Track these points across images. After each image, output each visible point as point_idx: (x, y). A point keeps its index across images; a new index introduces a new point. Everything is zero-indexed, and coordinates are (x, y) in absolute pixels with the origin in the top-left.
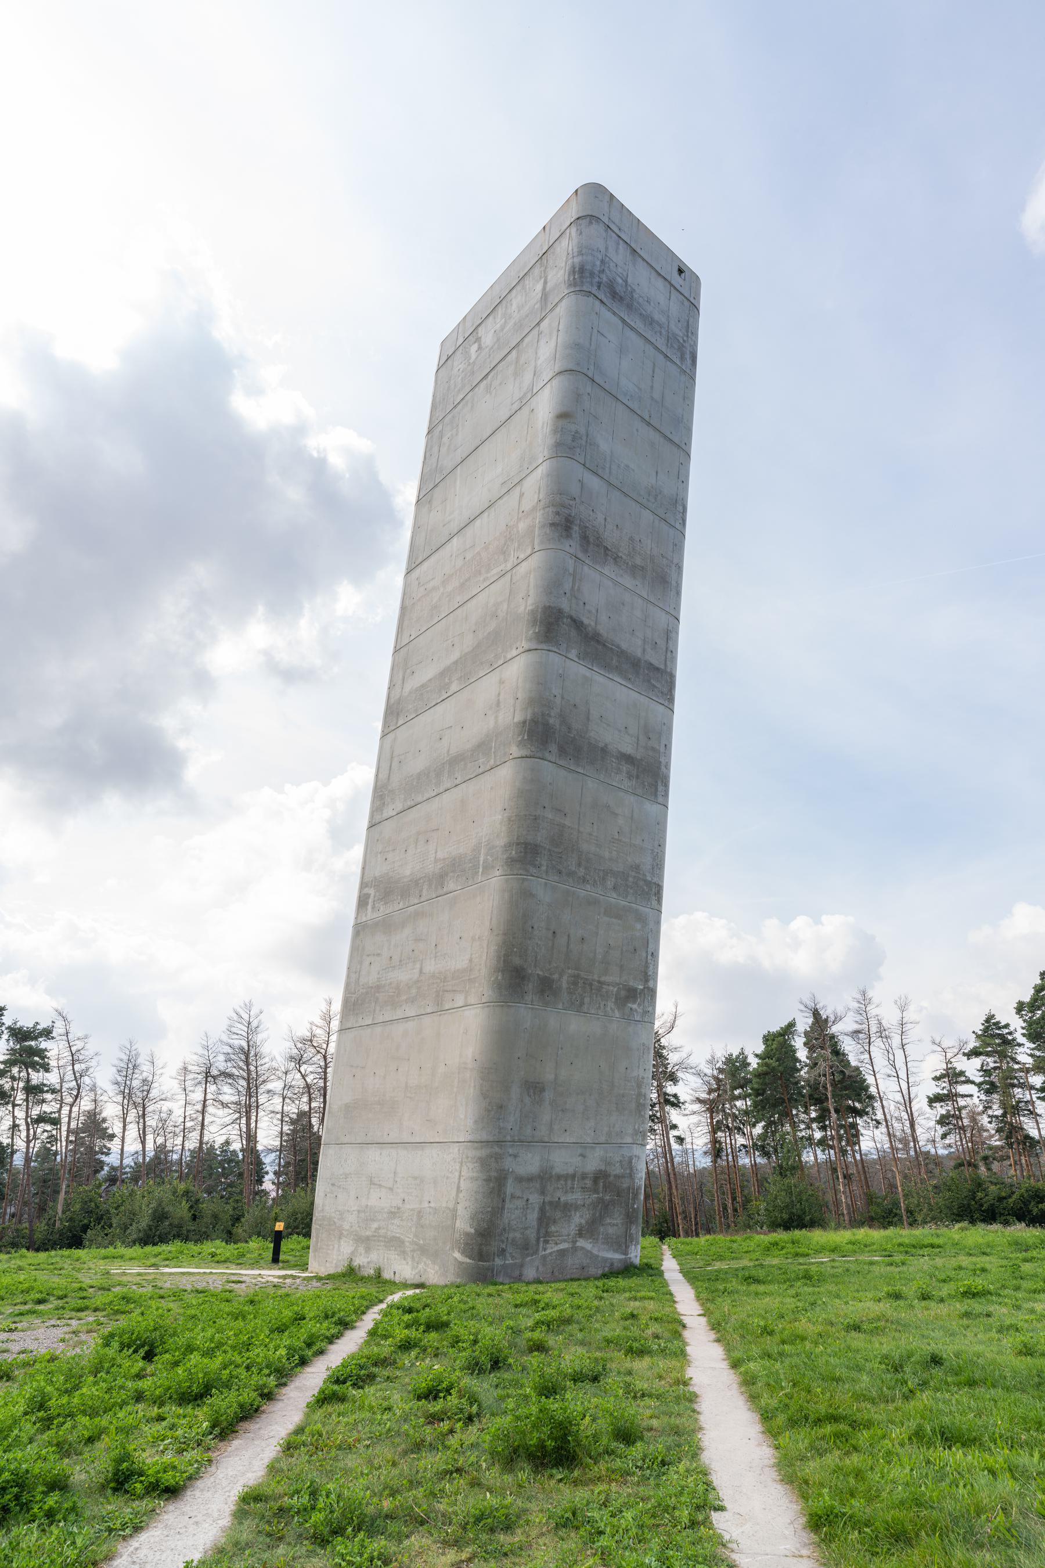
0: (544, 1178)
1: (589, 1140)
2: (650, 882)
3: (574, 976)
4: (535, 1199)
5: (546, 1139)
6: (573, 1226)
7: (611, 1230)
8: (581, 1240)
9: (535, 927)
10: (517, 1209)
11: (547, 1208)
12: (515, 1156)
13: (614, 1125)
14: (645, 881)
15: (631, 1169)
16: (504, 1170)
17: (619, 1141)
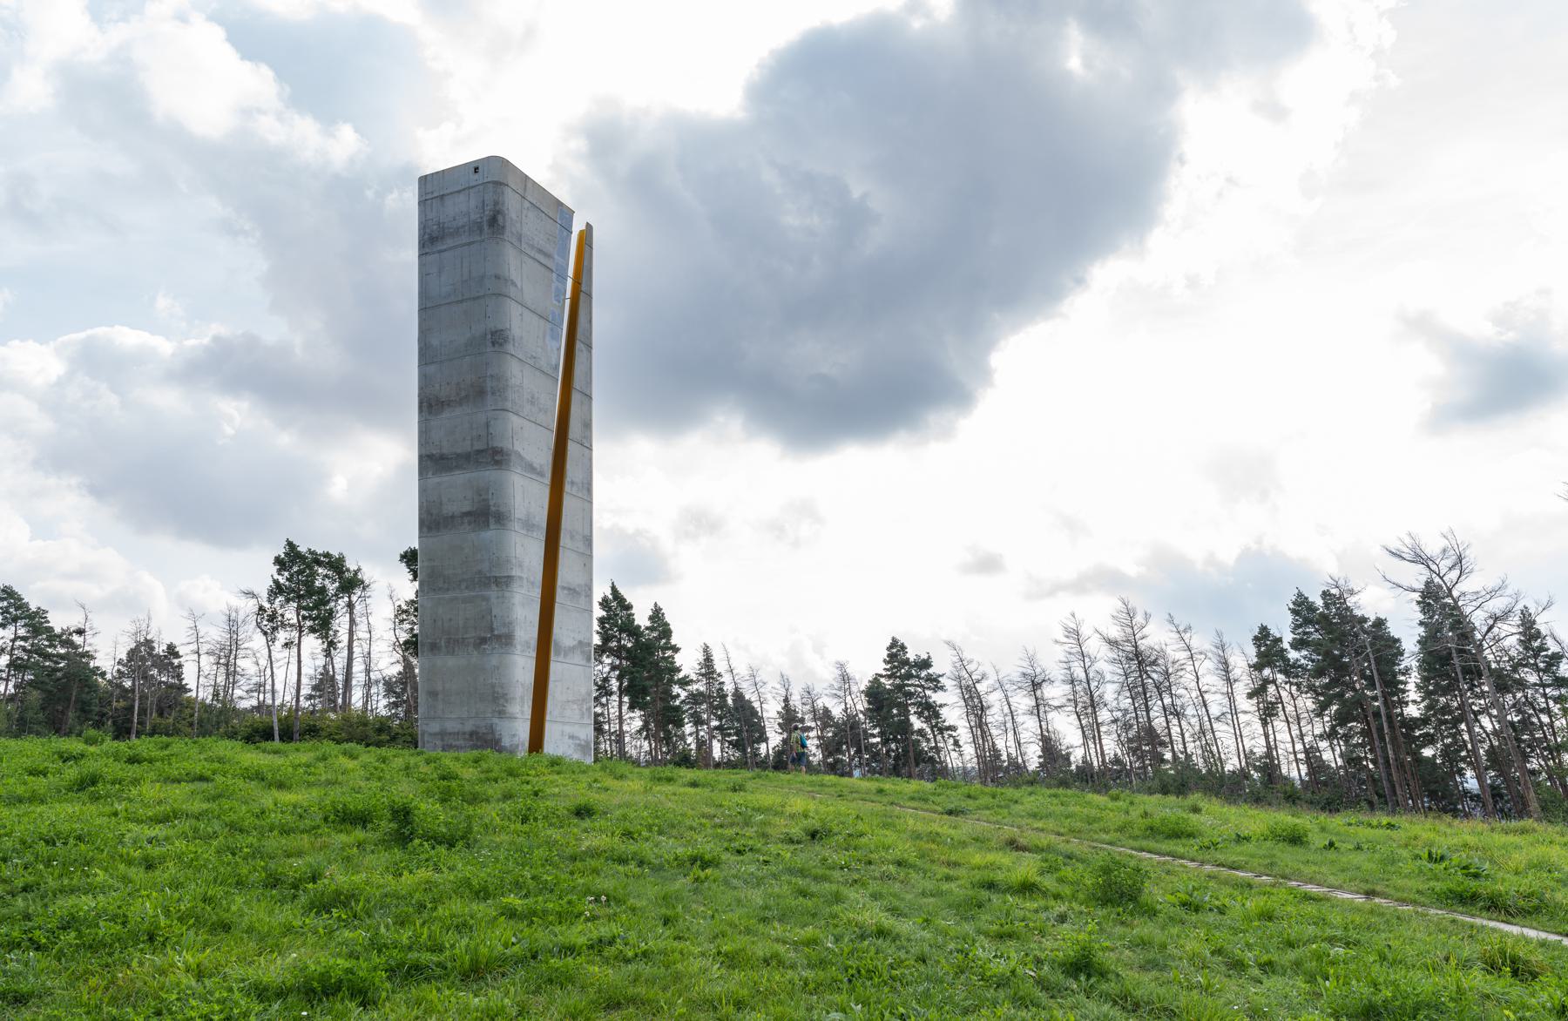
14: (486, 578)
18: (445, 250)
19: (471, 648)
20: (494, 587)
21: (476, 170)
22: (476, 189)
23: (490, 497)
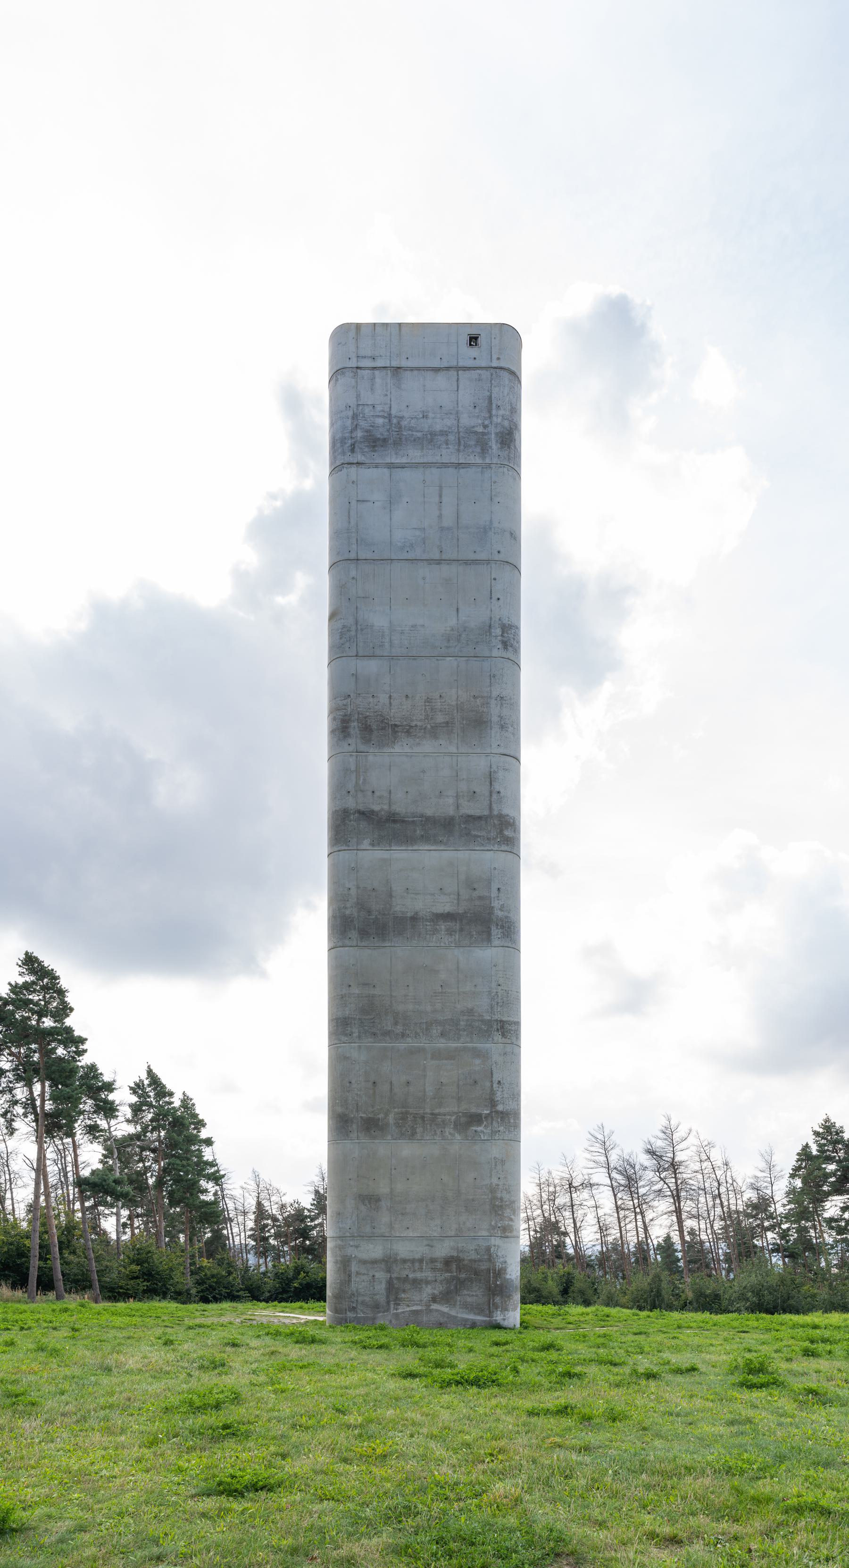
0: (389, 1262)
1: (435, 1234)
2: (490, 1021)
3: (402, 1113)
4: (381, 1275)
5: (387, 1235)
6: (425, 1295)
7: (469, 1299)
8: (435, 1305)
9: (353, 1082)
10: (363, 1281)
11: (395, 1282)
12: (357, 1247)
13: (464, 1223)
14: (483, 1021)
15: (490, 1255)
16: (347, 1256)
17: (472, 1234)
18: (402, 467)
19: (448, 1130)
20: (498, 1037)
21: (473, 340)
22: (474, 374)
23: (494, 894)
